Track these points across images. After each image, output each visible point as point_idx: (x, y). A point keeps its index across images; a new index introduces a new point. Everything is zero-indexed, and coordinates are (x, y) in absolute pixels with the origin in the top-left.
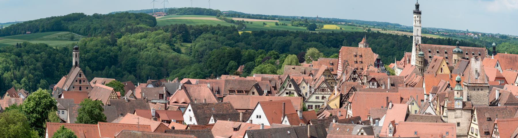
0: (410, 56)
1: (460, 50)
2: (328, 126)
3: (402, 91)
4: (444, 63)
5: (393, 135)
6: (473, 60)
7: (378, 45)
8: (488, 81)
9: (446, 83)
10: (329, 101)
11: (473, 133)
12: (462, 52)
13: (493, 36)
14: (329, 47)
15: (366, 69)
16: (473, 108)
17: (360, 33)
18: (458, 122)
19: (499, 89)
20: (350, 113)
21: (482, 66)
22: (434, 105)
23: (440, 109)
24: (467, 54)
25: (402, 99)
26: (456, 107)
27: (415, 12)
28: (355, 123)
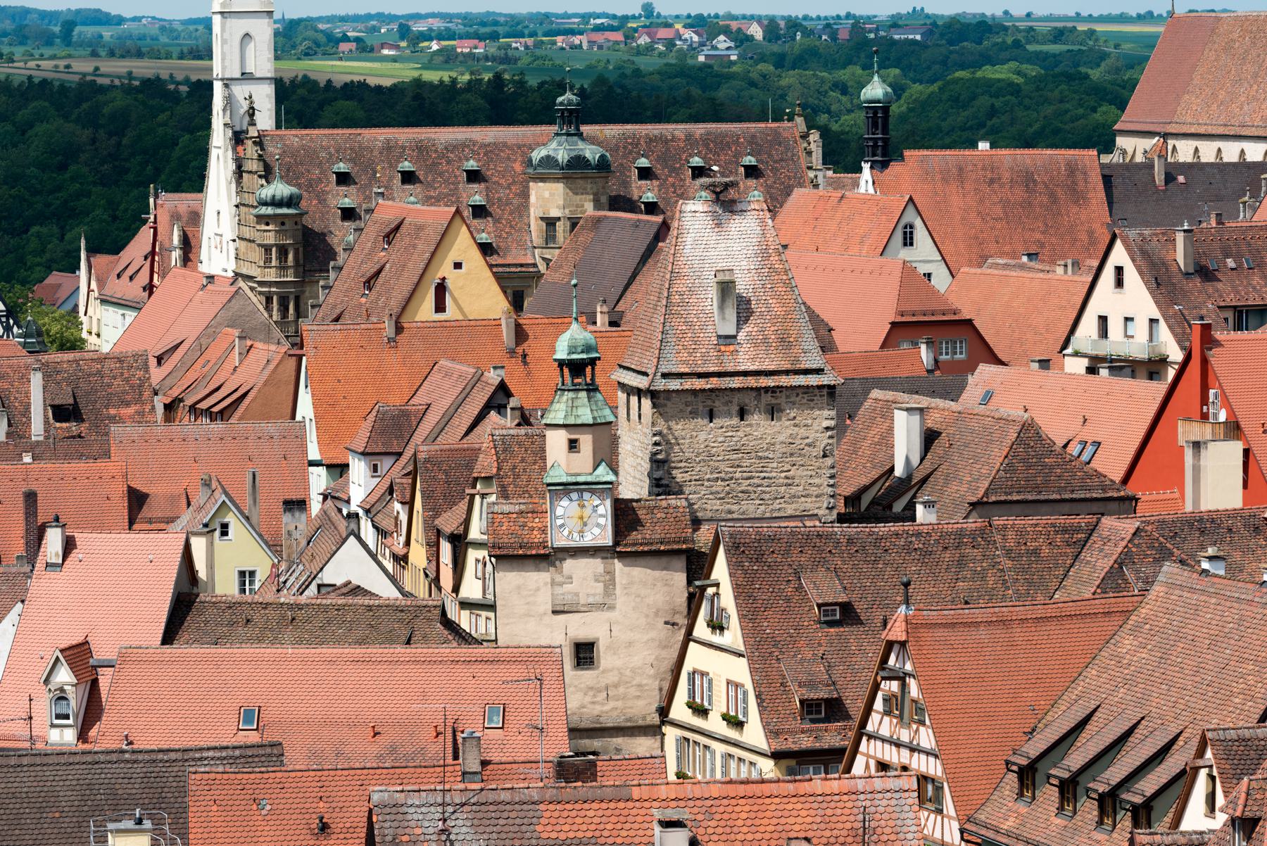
0: (196, 218)
1: (591, 153)
4: (463, 246)
5: (82, 736)
6: (694, 214)
8: (827, 347)
9: (479, 378)
11: (702, 712)
12: (603, 165)
18: (584, 635)
19: (924, 401)
21: (774, 255)
22: (381, 532)
23: (435, 556)
24: (645, 173)
25: (137, 500)
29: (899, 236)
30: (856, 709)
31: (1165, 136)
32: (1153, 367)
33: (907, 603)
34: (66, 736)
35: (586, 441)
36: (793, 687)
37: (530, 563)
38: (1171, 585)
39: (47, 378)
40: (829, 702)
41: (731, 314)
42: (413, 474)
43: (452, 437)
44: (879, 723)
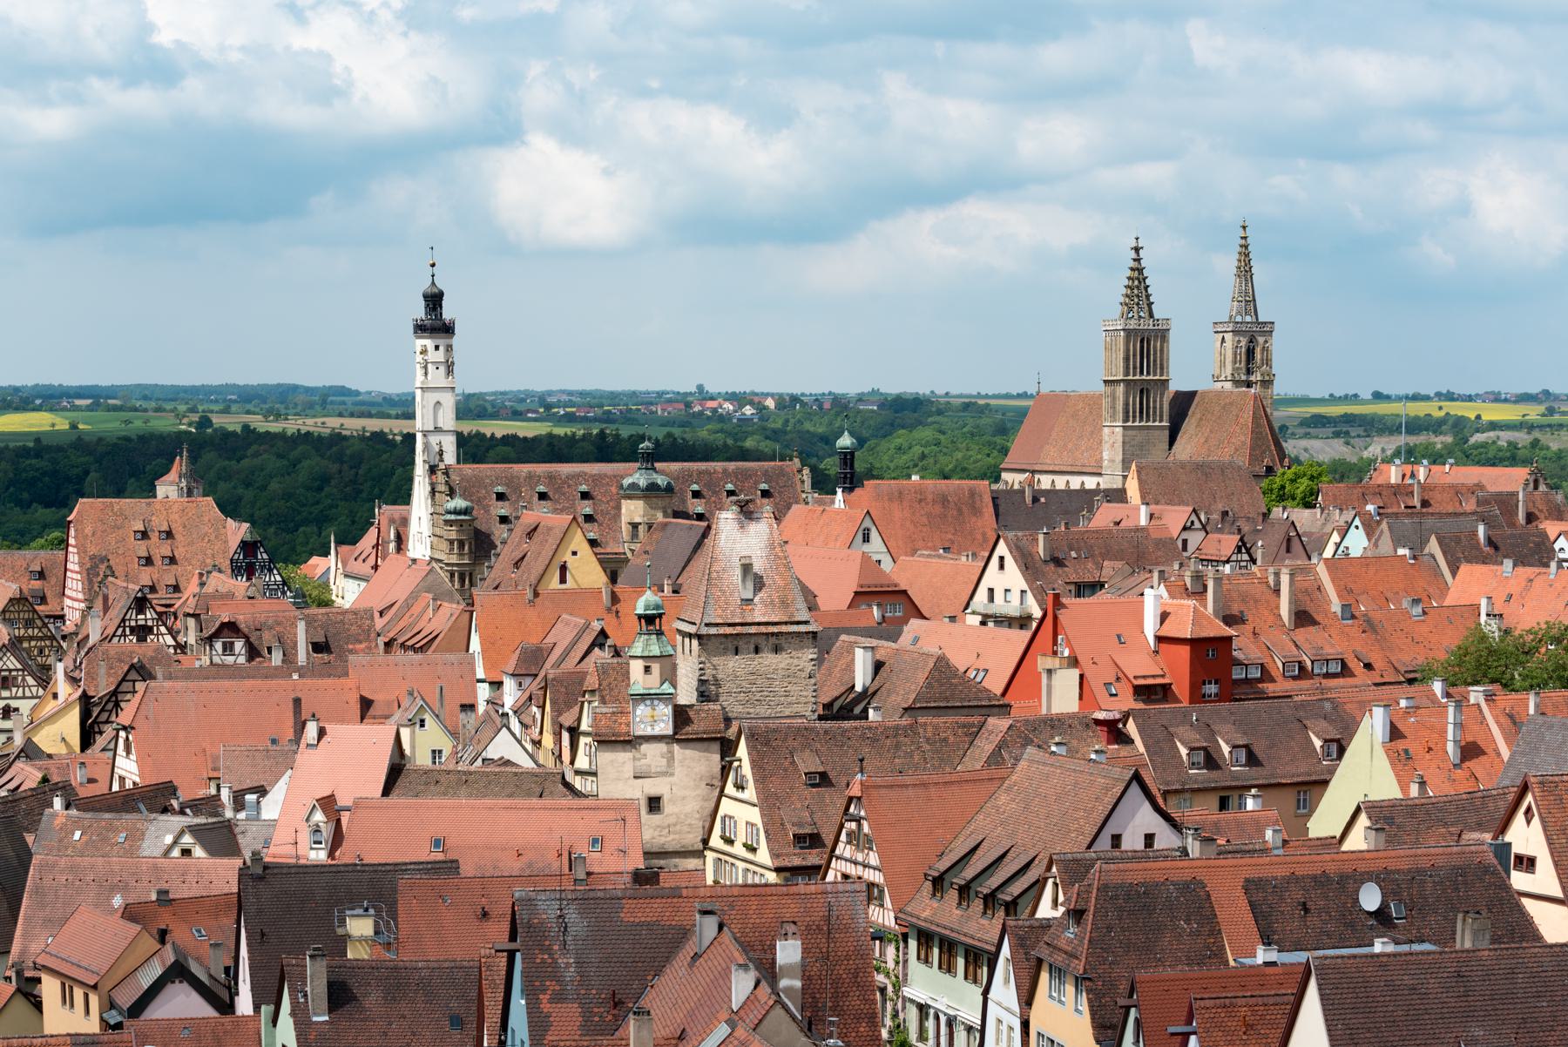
0: (405, 522)
1: (661, 481)
2: (33, 826)
3: (367, 669)
4: (578, 541)
5: (331, 855)
6: (726, 520)
7: (248, 485)
10: (34, 725)
11: (730, 842)
12: (669, 489)
13: (840, 405)
14: (25, 505)
15: (191, 588)
16: (731, 733)
17: (161, 438)
18: (654, 792)
19: (874, 642)
20: (129, 769)
21: (779, 548)
22: (524, 726)
23: (558, 741)
24: (696, 494)
25: (366, 704)
26: (641, 730)
27: (421, 329)
28: (151, 810)
29: (860, 536)
30: (829, 841)
31: (1033, 472)
32: (1023, 621)
33: (862, 771)
34: (319, 856)
35: (656, 668)
36: (788, 826)
37: (620, 746)
38: (1031, 761)
39: (308, 624)
40: (812, 836)
41: (750, 585)
42: (545, 688)
43: (570, 664)
44: (843, 849)
